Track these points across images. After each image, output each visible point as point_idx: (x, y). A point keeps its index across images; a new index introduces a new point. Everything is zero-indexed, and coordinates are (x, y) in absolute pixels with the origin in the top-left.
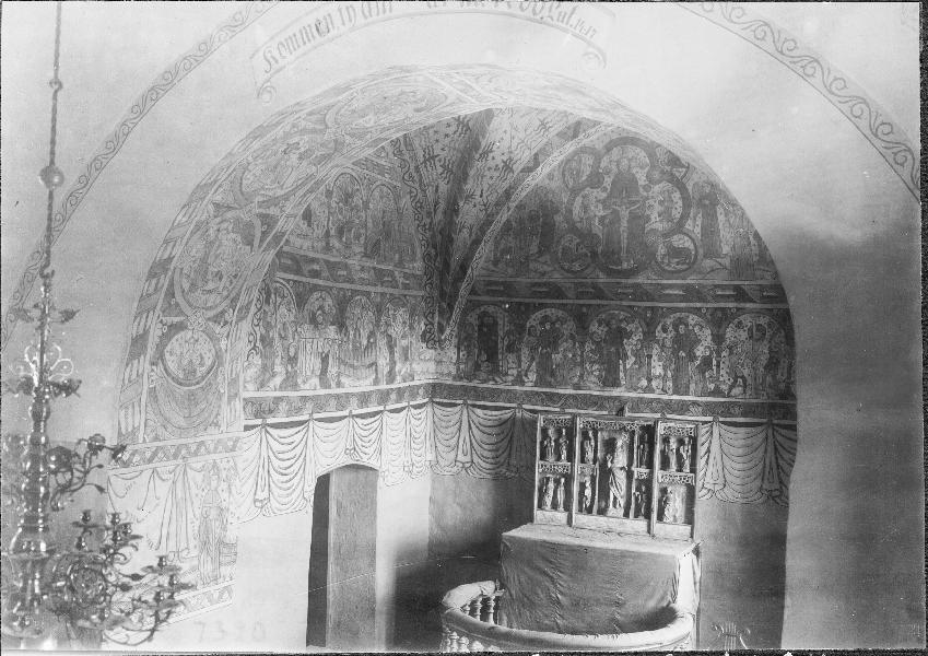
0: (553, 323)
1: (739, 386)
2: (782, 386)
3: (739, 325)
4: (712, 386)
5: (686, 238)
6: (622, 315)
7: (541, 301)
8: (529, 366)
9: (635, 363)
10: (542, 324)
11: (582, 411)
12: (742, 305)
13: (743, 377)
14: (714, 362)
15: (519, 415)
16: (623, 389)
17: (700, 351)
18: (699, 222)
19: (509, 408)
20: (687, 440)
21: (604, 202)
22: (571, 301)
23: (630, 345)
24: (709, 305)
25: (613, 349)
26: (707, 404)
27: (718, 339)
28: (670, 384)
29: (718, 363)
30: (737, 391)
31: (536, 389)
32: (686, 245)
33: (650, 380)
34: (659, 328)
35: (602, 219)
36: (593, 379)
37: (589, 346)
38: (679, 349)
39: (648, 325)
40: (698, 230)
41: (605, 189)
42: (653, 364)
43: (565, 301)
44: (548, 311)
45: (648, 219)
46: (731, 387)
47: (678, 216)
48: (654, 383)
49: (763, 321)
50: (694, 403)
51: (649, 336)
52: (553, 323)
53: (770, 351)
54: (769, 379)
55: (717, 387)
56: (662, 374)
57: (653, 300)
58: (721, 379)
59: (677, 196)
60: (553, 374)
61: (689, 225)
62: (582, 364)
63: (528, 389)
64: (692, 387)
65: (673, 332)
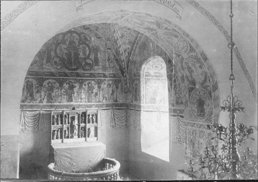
0: (52, 84)
2: (115, 99)
3: (105, 84)
4: (98, 100)
5: (90, 60)
7: (48, 77)
8: (44, 97)
9: (77, 95)
10: (48, 84)
11: (89, 109)
13: (106, 98)
14: (98, 94)
15: (41, 112)
16: (74, 102)
17: (95, 91)
18: (93, 56)
19: (38, 110)
20: (94, 115)
21: (66, 48)
22: (57, 77)
23: (75, 90)
24: (97, 79)
25: (70, 91)
26: (97, 105)
27: (99, 87)
28: (87, 100)
29: (99, 94)
30: (104, 101)
31: (47, 104)
32: (90, 62)
33: (81, 99)
34: (84, 85)
35: (66, 54)
36: (65, 100)
37: (63, 90)
38: (89, 90)
40: (93, 58)
41: (66, 45)
43: (55, 77)
44: (50, 80)
45: (79, 54)
46: (103, 100)
47: (88, 54)
48: (82, 100)
49: (110, 82)
50: (93, 105)
51: (81, 87)
52: (52, 84)
53: (112, 90)
54: (112, 97)
55: (99, 100)
56: (85, 97)
57: (82, 77)
58: (100, 98)
59: (87, 49)
60: (52, 99)
61: (91, 57)
62: (61, 96)
63: (44, 104)
64: (93, 100)
65: (88, 86)
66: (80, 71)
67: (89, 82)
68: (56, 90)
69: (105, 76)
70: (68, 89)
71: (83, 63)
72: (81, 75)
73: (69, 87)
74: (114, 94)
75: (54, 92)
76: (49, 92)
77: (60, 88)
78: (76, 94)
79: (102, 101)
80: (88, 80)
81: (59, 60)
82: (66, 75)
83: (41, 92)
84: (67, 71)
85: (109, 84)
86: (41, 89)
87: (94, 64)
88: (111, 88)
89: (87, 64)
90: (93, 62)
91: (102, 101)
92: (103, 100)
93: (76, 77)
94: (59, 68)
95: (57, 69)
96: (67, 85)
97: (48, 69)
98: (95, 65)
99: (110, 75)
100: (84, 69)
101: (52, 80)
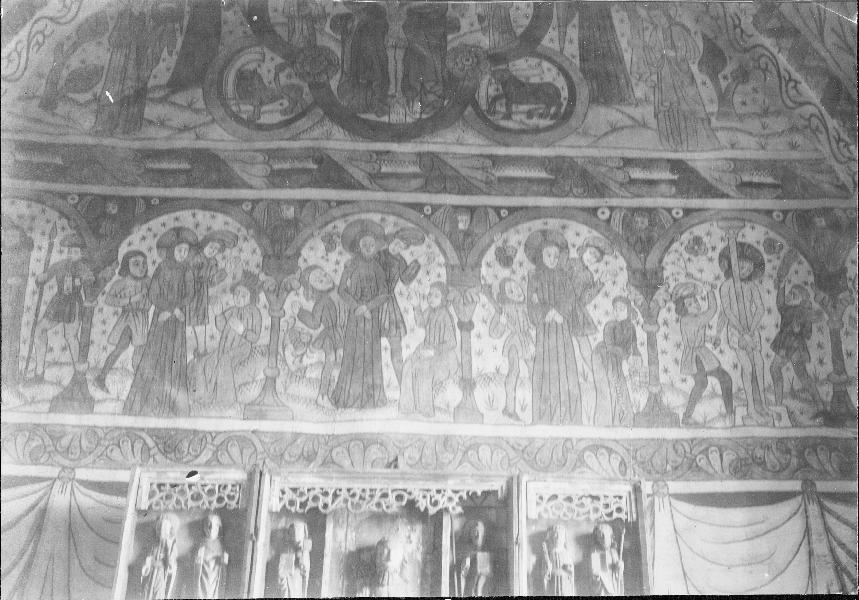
0: (197, 247)
1: (713, 395)
2: (826, 392)
4: (640, 399)
5: (546, 65)
6: (391, 225)
8: (112, 359)
9: (426, 343)
10: (166, 246)
12: (695, 203)
13: (721, 373)
14: (641, 336)
15: (60, 500)
16: (390, 412)
17: (602, 311)
18: (573, 33)
20: (607, 532)
23: (410, 299)
24: (614, 202)
25: (364, 309)
26: (634, 447)
27: (648, 281)
28: (525, 394)
30: (710, 407)
31: (128, 421)
33: (467, 385)
34: (490, 255)
36: (310, 392)
37: (296, 301)
38: (545, 305)
39: (458, 248)
40: (572, 49)
42: (475, 344)
44: (186, 218)
46: (694, 399)
47: (526, 22)
48: (480, 395)
50: (596, 447)
51: (462, 273)
52: (197, 247)
53: (783, 309)
54: (789, 374)
55: (655, 401)
56: (505, 371)
58: (663, 378)
60: (185, 379)
61: (549, 40)
62: (272, 351)
64: (588, 401)
65: (529, 267)
66: (459, 144)
67: (544, 233)
68: (229, 299)
69: (688, 180)
70: (343, 291)
71: (487, 88)
72: (464, 172)
73: (349, 270)
74: (812, 343)
75: (214, 311)
76: (165, 316)
77: (270, 282)
78: (421, 333)
79: (688, 414)
80: (536, 213)
81: (280, 68)
82: (329, 172)
83: (86, 316)
84: (339, 143)
85: (745, 251)
86: (96, 286)
87: (583, 93)
88: (769, 284)
89: (515, 91)
90: (577, 76)
91: (688, 414)
92: (694, 399)
93: (423, 189)
94: (277, 118)
95: (260, 127)
96: (333, 256)
97: (185, 128)
98: (594, 100)
99: (746, 178)
100: (498, 129)
101: (201, 215)
